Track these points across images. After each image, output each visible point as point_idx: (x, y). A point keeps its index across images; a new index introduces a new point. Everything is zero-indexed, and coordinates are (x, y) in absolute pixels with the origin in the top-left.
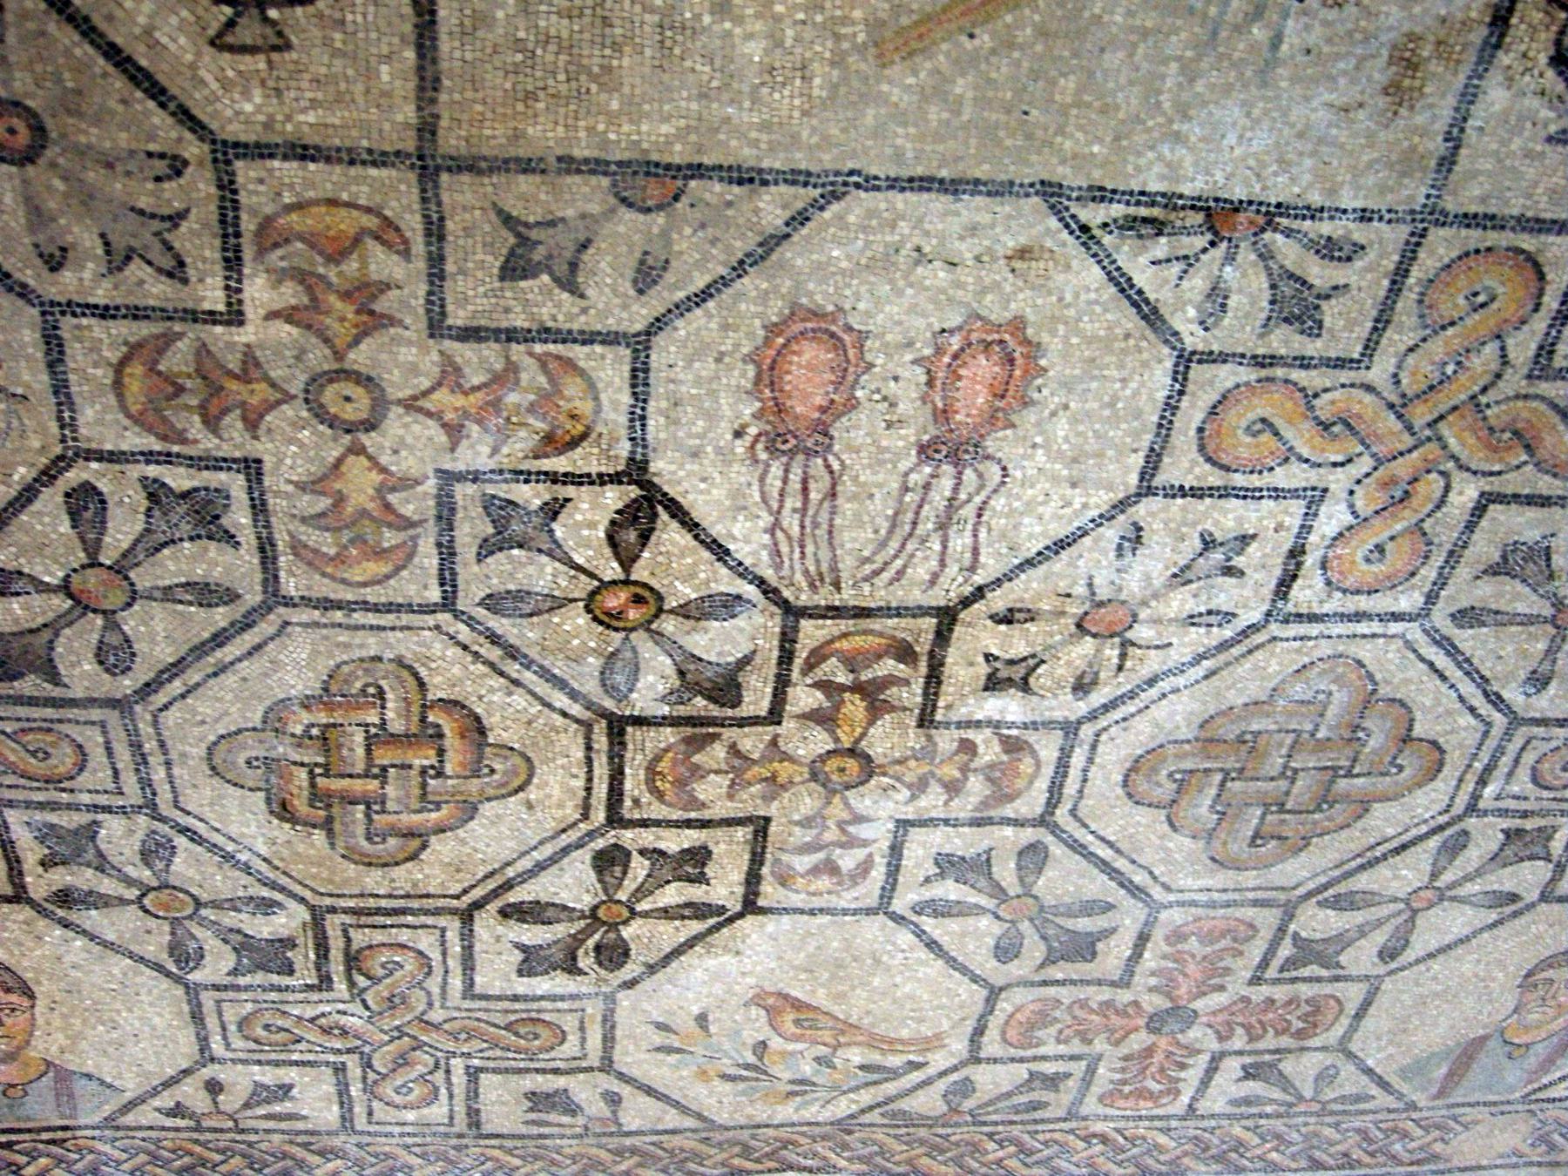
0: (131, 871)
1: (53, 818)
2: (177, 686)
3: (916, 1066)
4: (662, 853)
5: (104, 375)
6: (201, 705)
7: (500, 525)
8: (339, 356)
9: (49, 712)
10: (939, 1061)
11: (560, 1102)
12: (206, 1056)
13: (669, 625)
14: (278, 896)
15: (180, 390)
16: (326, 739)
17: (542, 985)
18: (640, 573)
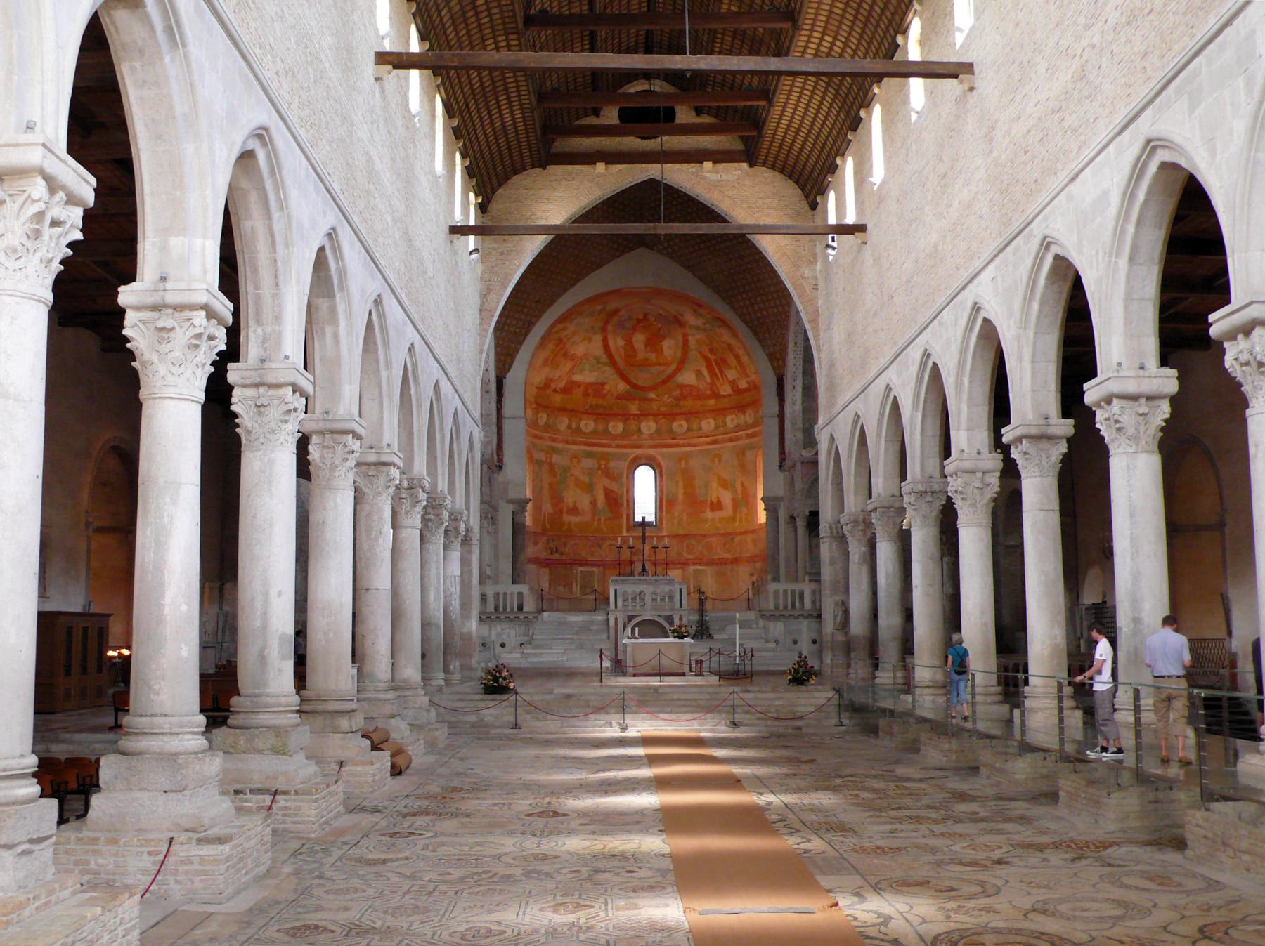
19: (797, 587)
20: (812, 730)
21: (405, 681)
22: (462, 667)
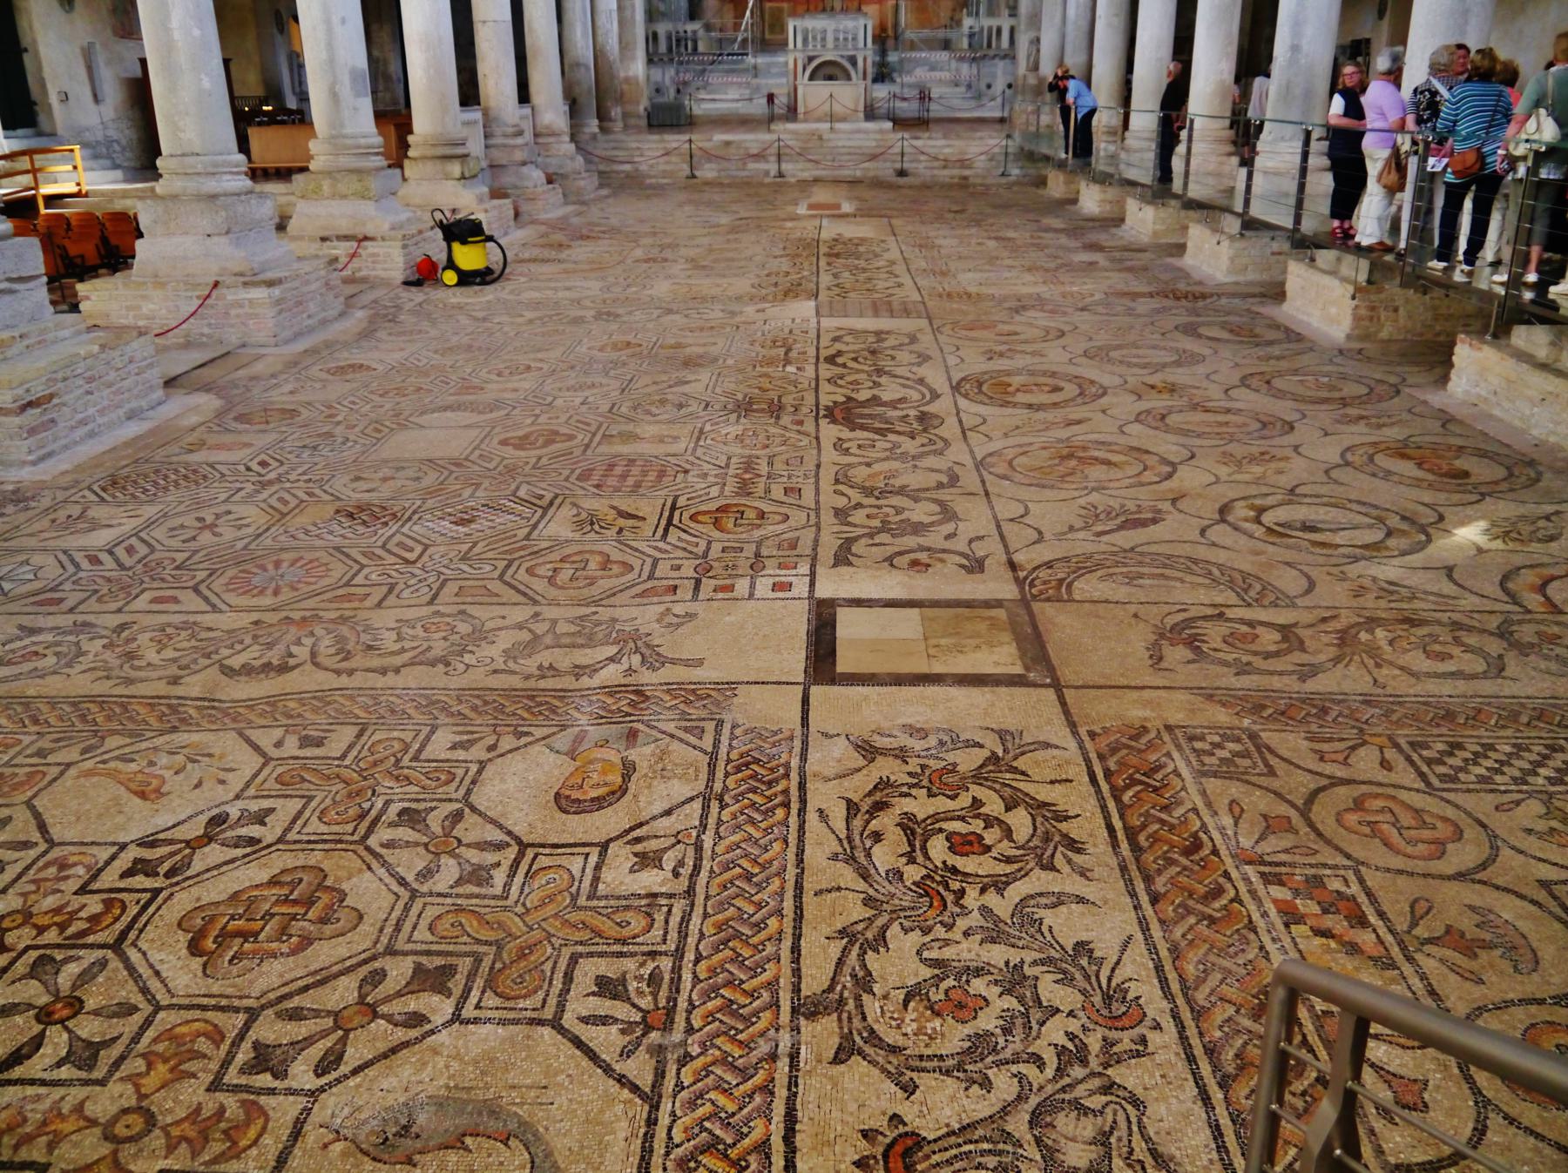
0: (452, 862)
1: (476, 890)
2: (348, 963)
3: (104, 762)
4: (147, 875)
5: (267, 1140)
6: (343, 951)
7: (95, 1056)
8: (115, 1152)
9: (434, 947)
10: (89, 764)
11: (306, 742)
12: (482, 765)
13: (44, 999)
14: (379, 850)
15: (225, 1132)
16: (283, 932)
17: (266, 804)
18: (38, 1028)
19: (994, 22)
20: (979, 181)
21: (547, 127)
22: (625, 115)
